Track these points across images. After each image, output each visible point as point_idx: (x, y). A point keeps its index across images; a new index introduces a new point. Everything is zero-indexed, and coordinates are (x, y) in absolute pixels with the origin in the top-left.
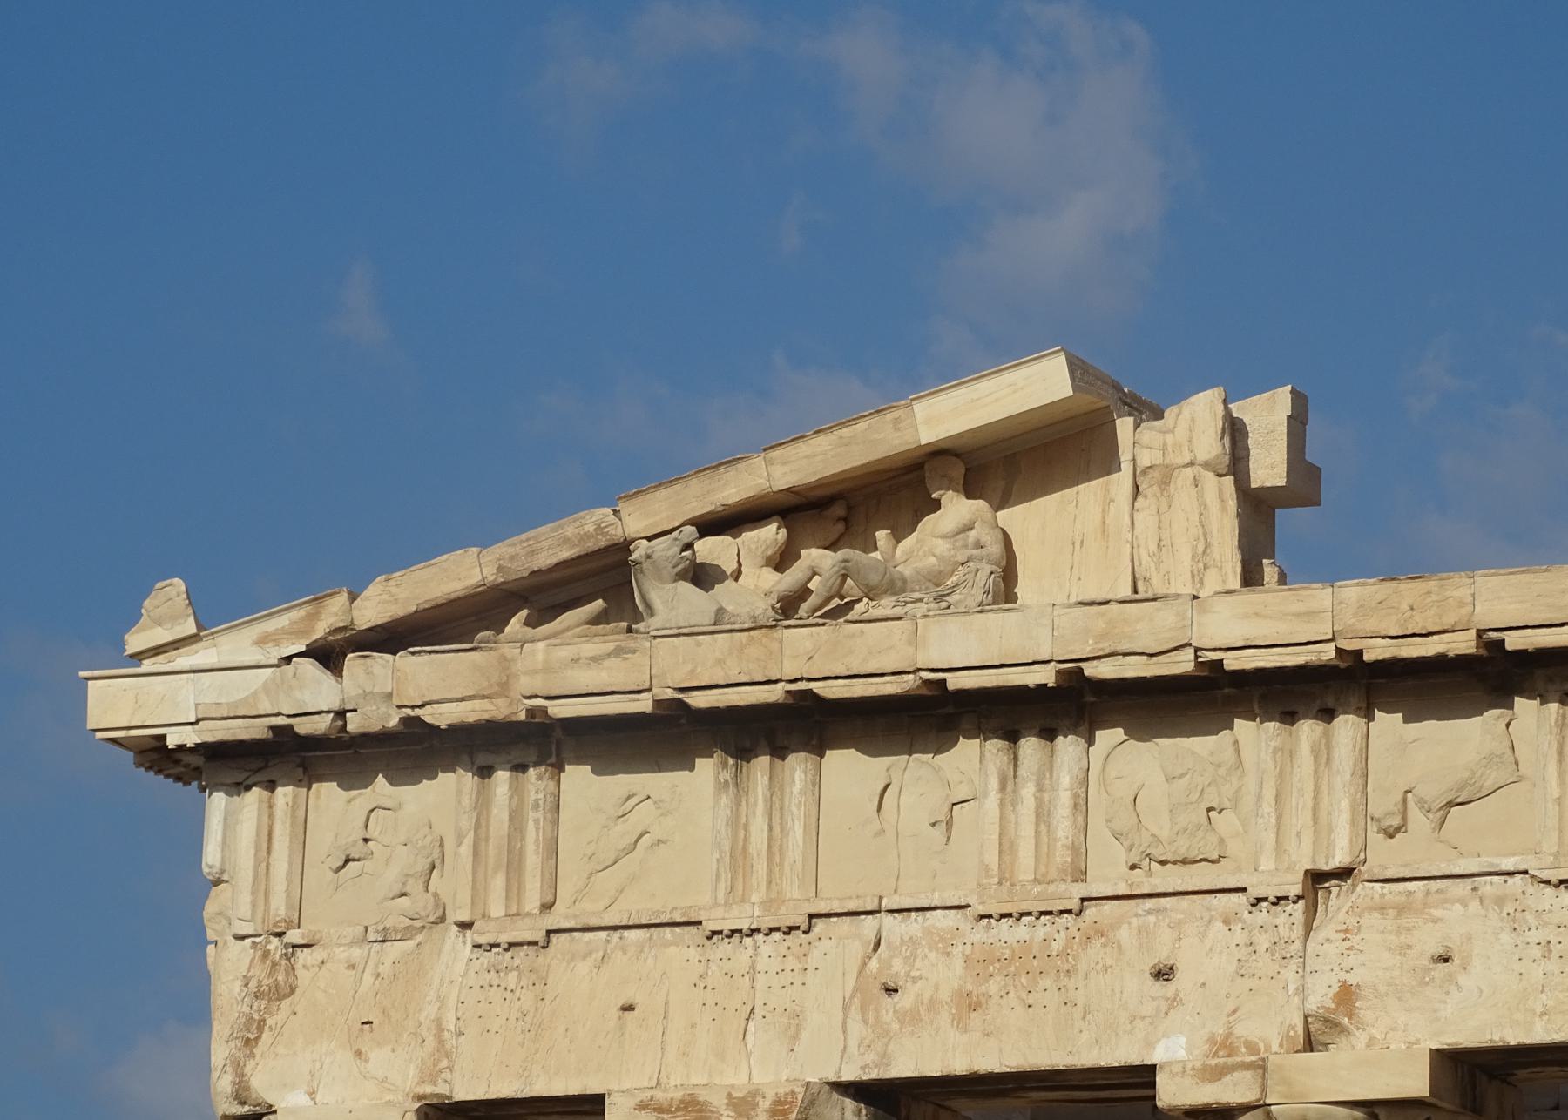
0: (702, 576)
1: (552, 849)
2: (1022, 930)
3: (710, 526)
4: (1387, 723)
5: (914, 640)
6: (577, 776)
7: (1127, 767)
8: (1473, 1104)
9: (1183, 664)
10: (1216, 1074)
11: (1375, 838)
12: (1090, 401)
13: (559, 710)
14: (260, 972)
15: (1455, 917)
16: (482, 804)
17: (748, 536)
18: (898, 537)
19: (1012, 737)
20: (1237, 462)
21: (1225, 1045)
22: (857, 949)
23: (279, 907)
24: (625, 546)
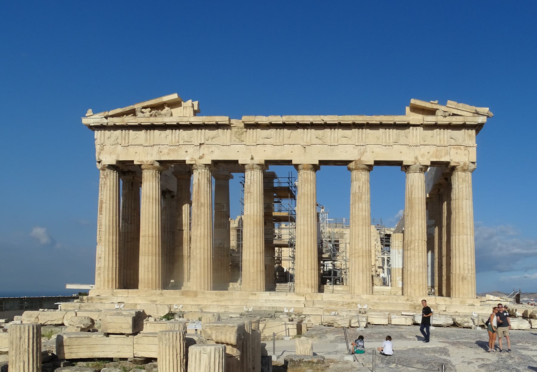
2: (173, 147)
3: (144, 108)
6: (131, 131)
10: (191, 161)
12: (179, 99)
15: (213, 148)
16: (122, 133)
21: (192, 158)
23: (102, 142)
24: (135, 109)
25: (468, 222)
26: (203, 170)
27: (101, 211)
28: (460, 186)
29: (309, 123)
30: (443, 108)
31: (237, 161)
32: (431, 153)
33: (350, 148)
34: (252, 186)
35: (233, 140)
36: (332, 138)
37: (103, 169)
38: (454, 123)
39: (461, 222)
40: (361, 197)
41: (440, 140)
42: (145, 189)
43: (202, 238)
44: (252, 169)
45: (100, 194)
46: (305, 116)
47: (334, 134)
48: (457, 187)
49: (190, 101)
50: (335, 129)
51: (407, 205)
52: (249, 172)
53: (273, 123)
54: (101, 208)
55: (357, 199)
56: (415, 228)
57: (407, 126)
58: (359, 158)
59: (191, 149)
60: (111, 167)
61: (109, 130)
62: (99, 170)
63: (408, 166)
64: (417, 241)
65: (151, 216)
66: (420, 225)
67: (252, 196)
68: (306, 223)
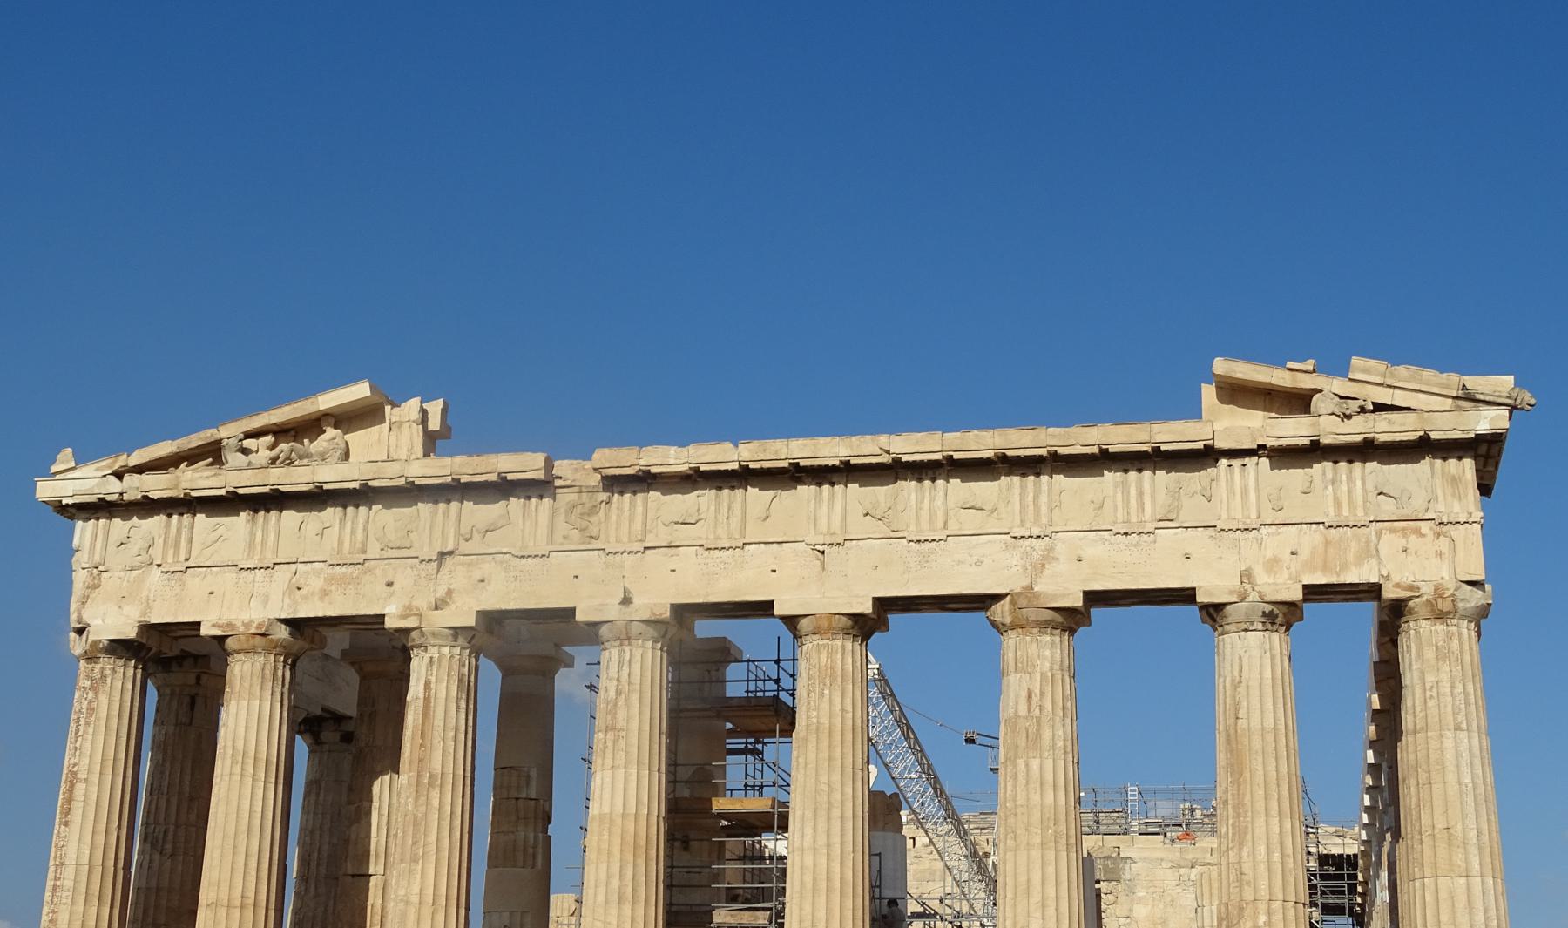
0: (245, 451)
1: (190, 541)
2: (344, 569)
3: (248, 435)
4: (468, 505)
5: (313, 473)
6: (200, 517)
7: (381, 517)
8: (490, 631)
9: (401, 482)
10: (404, 617)
11: (462, 542)
12: (377, 399)
13: (195, 494)
14: (89, 580)
15: (487, 568)
16: (168, 526)
17: (262, 440)
18: (311, 441)
19: (345, 507)
20: (424, 419)
21: (409, 608)
22: (289, 575)
23: (97, 558)
25: (1471, 823)
26: (446, 650)
27: (68, 812)
28: (1430, 678)
29: (836, 462)
30: (1338, 385)
31: (573, 611)
32: (1305, 553)
33: (990, 548)
34: (621, 703)
35: (558, 538)
36: (925, 514)
37: (90, 657)
38: (1382, 438)
39: (1440, 825)
40: (1038, 734)
41: (1337, 503)
42: (231, 724)
43: (427, 911)
44: (625, 638)
45: (70, 746)
46: (822, 440)
47: (932, 500)
48: (1416, 681)
49: (412, 406)
50: (933, 480)
51: (1222, 757)
52: (615, 652)
53: (703, 468)
54: (70, 799)
55: (1022, 743)
56: (1253, 853)
57: (1206, 456)
58: (1026, 582)
59: (405, 576)
60: (119, 648)
61: (126, 518)
62: (78, 659)
63: (1219, 607)
64: (1262, 907)
65: (244, 827)
66: (1275, 839)
67: (622, 743)
68: (822, 840)
